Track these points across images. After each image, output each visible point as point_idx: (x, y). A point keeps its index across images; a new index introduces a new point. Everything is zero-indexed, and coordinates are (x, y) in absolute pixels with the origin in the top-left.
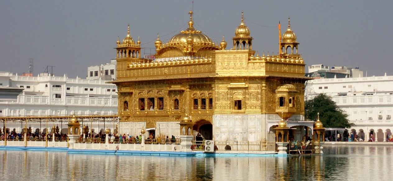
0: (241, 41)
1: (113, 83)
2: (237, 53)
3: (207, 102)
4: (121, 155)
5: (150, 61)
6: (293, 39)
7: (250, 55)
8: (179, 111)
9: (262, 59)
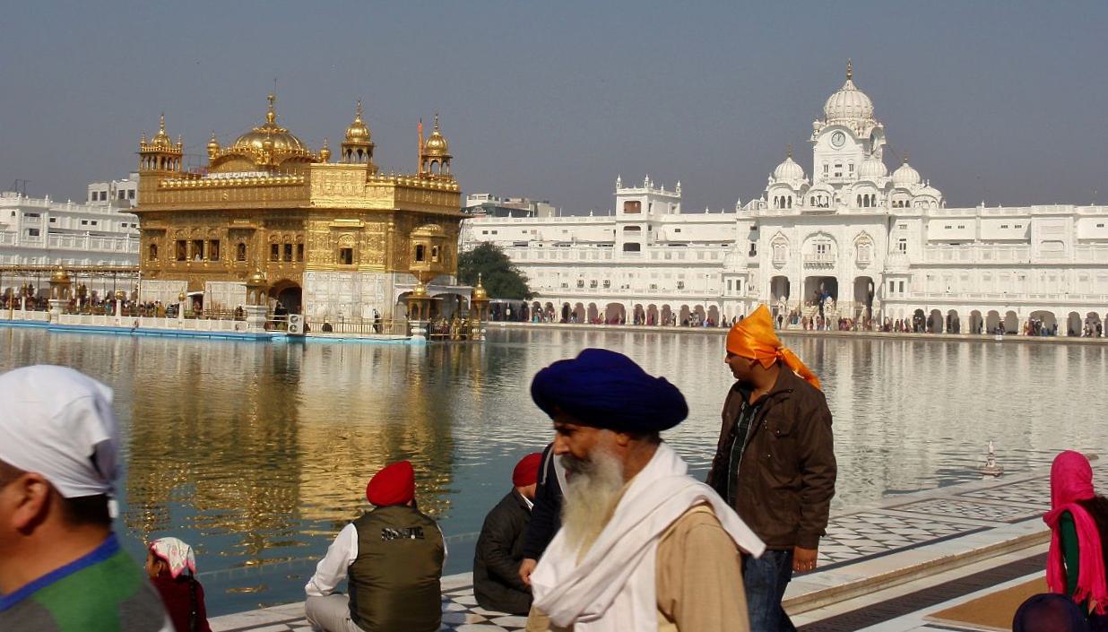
0: (355, 150)
1: (133, 213)
2: (348, 168)
3: (294, 250)
4: (143, 336)
5: (198, 177)
6: (442, 149)
7: (369, 173)
8: (245, 264)
9: (390, 181)
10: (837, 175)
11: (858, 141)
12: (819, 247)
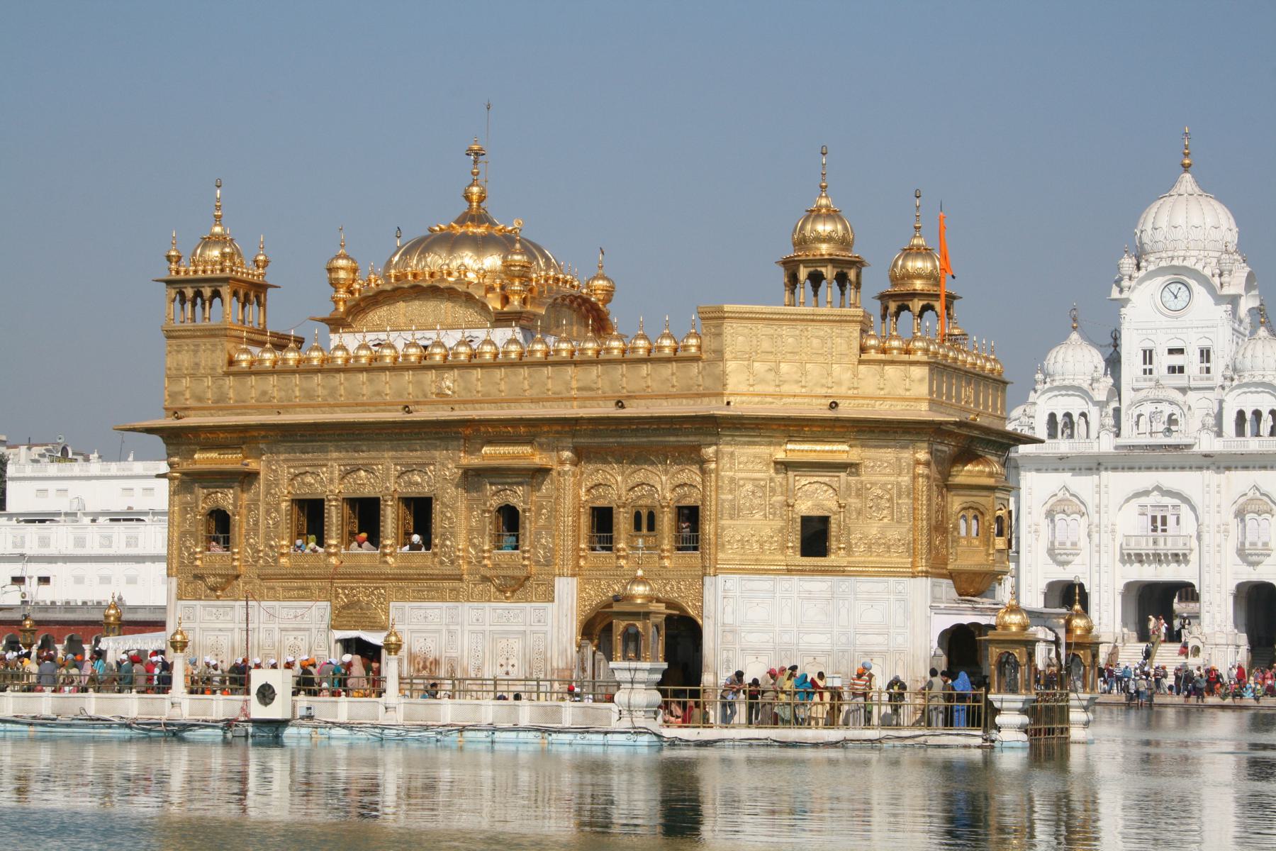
3: (666, 521)
10: (1172, 369)
11: (1219, 299)
12: (1154, 519)
